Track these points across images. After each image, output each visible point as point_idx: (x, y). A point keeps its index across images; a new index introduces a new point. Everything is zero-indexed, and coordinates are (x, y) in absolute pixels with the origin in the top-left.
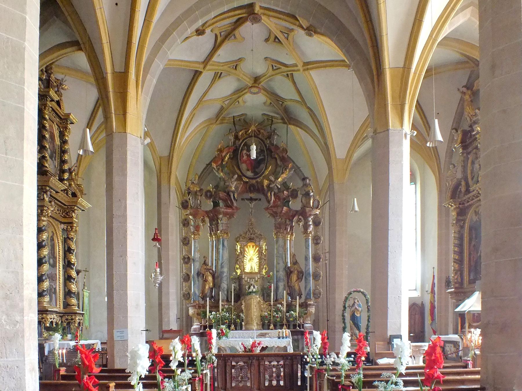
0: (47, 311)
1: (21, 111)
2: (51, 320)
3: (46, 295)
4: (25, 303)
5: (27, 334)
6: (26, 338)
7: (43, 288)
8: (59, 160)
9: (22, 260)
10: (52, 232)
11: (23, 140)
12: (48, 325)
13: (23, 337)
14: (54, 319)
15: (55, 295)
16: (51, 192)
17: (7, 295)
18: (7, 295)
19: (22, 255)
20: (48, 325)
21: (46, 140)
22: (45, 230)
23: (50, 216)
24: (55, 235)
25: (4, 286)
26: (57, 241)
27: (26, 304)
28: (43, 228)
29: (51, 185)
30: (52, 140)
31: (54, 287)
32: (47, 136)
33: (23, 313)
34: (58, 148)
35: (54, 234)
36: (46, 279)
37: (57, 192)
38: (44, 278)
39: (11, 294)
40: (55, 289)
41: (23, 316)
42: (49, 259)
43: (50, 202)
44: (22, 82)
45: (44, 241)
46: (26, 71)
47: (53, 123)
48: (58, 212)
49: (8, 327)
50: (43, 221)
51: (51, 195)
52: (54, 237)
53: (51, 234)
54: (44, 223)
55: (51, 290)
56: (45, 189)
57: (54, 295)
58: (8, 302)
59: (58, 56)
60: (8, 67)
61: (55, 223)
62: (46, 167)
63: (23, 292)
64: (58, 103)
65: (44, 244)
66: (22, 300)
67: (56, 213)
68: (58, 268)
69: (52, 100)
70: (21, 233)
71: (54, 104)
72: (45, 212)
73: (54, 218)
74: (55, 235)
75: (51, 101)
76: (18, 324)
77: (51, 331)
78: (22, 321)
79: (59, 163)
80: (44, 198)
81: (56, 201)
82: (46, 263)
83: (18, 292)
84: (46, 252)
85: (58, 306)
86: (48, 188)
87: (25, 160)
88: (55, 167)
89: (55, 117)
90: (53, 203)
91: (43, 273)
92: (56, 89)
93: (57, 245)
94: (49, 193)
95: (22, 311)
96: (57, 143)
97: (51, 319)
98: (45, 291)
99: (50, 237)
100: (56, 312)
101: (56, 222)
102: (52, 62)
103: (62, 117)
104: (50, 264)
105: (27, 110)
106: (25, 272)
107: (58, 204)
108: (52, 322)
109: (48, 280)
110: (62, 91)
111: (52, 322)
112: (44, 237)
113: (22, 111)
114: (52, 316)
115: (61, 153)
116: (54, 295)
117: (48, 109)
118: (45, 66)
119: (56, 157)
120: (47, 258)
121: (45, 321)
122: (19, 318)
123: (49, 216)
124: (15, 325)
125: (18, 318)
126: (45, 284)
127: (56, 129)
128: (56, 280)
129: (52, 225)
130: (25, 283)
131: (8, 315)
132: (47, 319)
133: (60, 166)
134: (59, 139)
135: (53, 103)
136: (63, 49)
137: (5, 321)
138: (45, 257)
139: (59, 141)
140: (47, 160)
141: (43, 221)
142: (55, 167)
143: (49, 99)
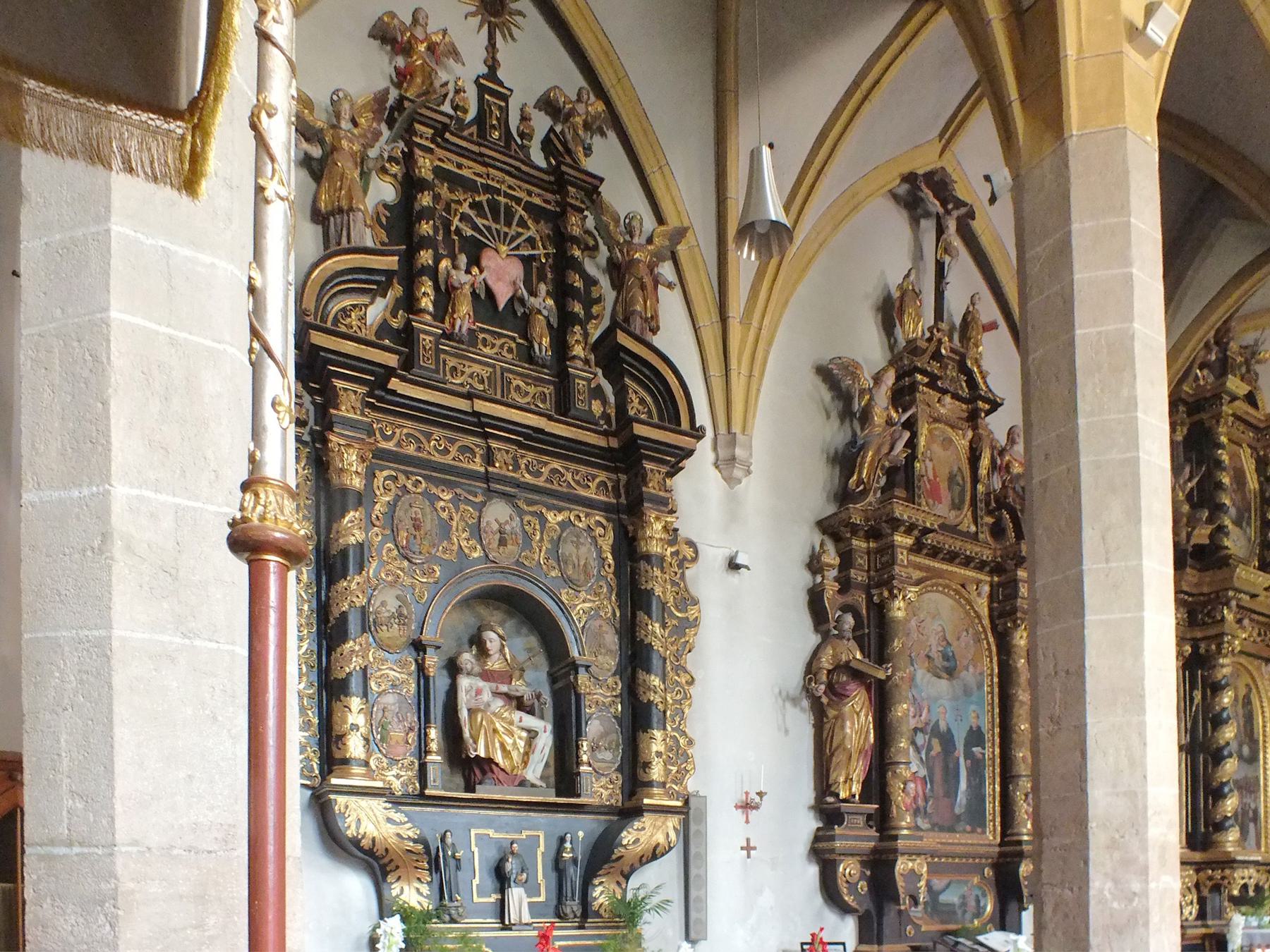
0: (1234, 861)
1: (1132, 466)
2: (1242, 882)
3: (1232, 826)
4: (1150, 854)
5: (1155, 919)
6: (1152, 927)
7: (1225, 811)
8: (1258, 523)
9: (1143, 766)
10: (1247, 685)
11: (1140, 521)
12: (1236, 892)
13: (1146, 924)
14: (1250, 878)
15: (1256, 824)
16: (1239, 600)
17: (1113, 840)
18: (1113, 840)
19: (1144, 756)
20: (1236, 892)
21: (1225, 490)
22: (1227, 685)
23: (1241, 652)
24: (1254, 690)
25: (1108, 824)
26: (1258, 703)
27: (1153, 857)
28: (1223, 682)
29: (1237, 584)
30: (1238, 484)
31: (1253, 806)
32: (1226, 480)
33: (1147, 874)
34: (1255, 497)
35: (1250, 690)
36: (1231, 790)
37: (1254, 596)
38: (1226, 789)
39: (1123, 837)
40: (1256, 812)
41: (1147, 882)
42: (1240, 746)
43: (1239, 621)
44: (1132, 403)
45: (1224, 709)
46: (1139, 380)
47: (1241, 446)
48: (1259, 639)
49: (1115, 905)
50: (1223, 666)
51: (1238, 606)
52: (1252, 696)
53: (1243, 692)
54: (1226, 671)
55: (1245, 813)
56: (1226, 596)
57: (1252, 826)
58: (1117, 855)
59: (1240, 298)
60: (1102, 391)
61: (1251, 664)
62: (1227, 548)
63: (1146, 832)
64: (1251, 399)
65: (1225, 715)
66: (1145, 849)
67: (1254, 641)
68: (1261, 762)
69: (1234, 398)
70: (1142, 710)
71: (1242, 407)
72: (1226, 645)
73: (1249, 655)
74: (1254, 690)
75: (1231, 402)
76: (1137, 899)
77: (1243, 905)
78: (1145, 893)
79: (1258, 530)
80: (1223, 617)
81: (1255, 617)
82: (1230, 756)
83: (1137, 834)
84: (1230, 732)
85: (1263, 849)
86: (1231, 593)
87: (1145, 562)
88: (1249, 540)
89: (1243, 433)
90: (1246, 622)
91: (1224, 780)
92: (1244, 370)
93: (1260, 712)
94: (1234, 603)
95: (1144, 871)
96: (1252, 487)
97: (1243, 878)
98: (1229, 818)
99: (1241, 698)
100: (1256, 863)
101: (1256, 662)
102: (1228, 314)
103: (1262, 425)
104: (1241, 757)
105: (1146, 457)
106: (1152, 790)
107: (1258, 622)
108: (1245, 887)
109: (1236, 792)
110: (1258, 368)
111: (1245, 887)
112: (1226, 700)
113: (1134, 463)
114: (1246, 873)
115: (1262, 506)
116: (1252, 826)
117: (1226, 423)
118: (1212, 333)
119: (1250, 518)
120: (1234, 746)
121: (1229, 883)
122: (1139, 885)
123: (1236, 651)
124: (1131, 901)
125: (1136, 886)
126: (1229, 802)
127: (1248, 455)
128: (1259, 790)
129: (1246, 668)
130: (1150, 813)
131: (1116, 881)
132: (1234, 879)
133: (1261, 535)
134: (1255, 476)
135: (1237, 403)
136: (1242, 283)
137: (1110, 893)
138: (1228, 744)
139: (1256, 482)
140: (1227, 534)
141: (1223, 666)
142: (1249, 540)
143: (1226, 398)
